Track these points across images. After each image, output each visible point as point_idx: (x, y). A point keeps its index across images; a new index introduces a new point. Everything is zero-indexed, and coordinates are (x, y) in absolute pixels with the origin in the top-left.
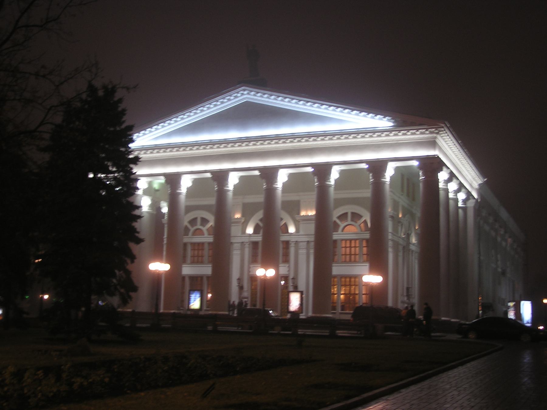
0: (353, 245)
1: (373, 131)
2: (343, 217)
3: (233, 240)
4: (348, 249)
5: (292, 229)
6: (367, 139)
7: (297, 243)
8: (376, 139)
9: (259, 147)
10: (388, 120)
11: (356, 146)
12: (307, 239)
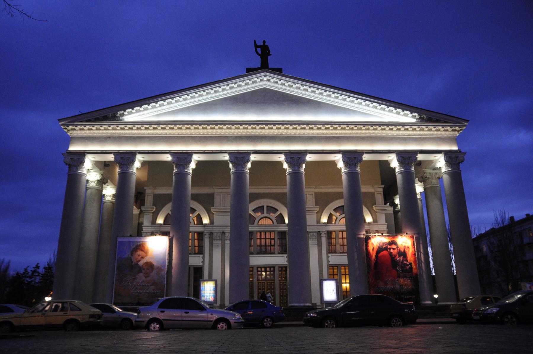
0: (268, 236)
1: (403, 125)
2: (260, 209)
3: (309, 229)
4: (263, 241)
5: (369, 219)
6: (395, 132)
7: (211, 234)
8: (402, 133)
9: (283, 131)
10: (414, 117)
11: (383, 137)
12: (152, 230)
